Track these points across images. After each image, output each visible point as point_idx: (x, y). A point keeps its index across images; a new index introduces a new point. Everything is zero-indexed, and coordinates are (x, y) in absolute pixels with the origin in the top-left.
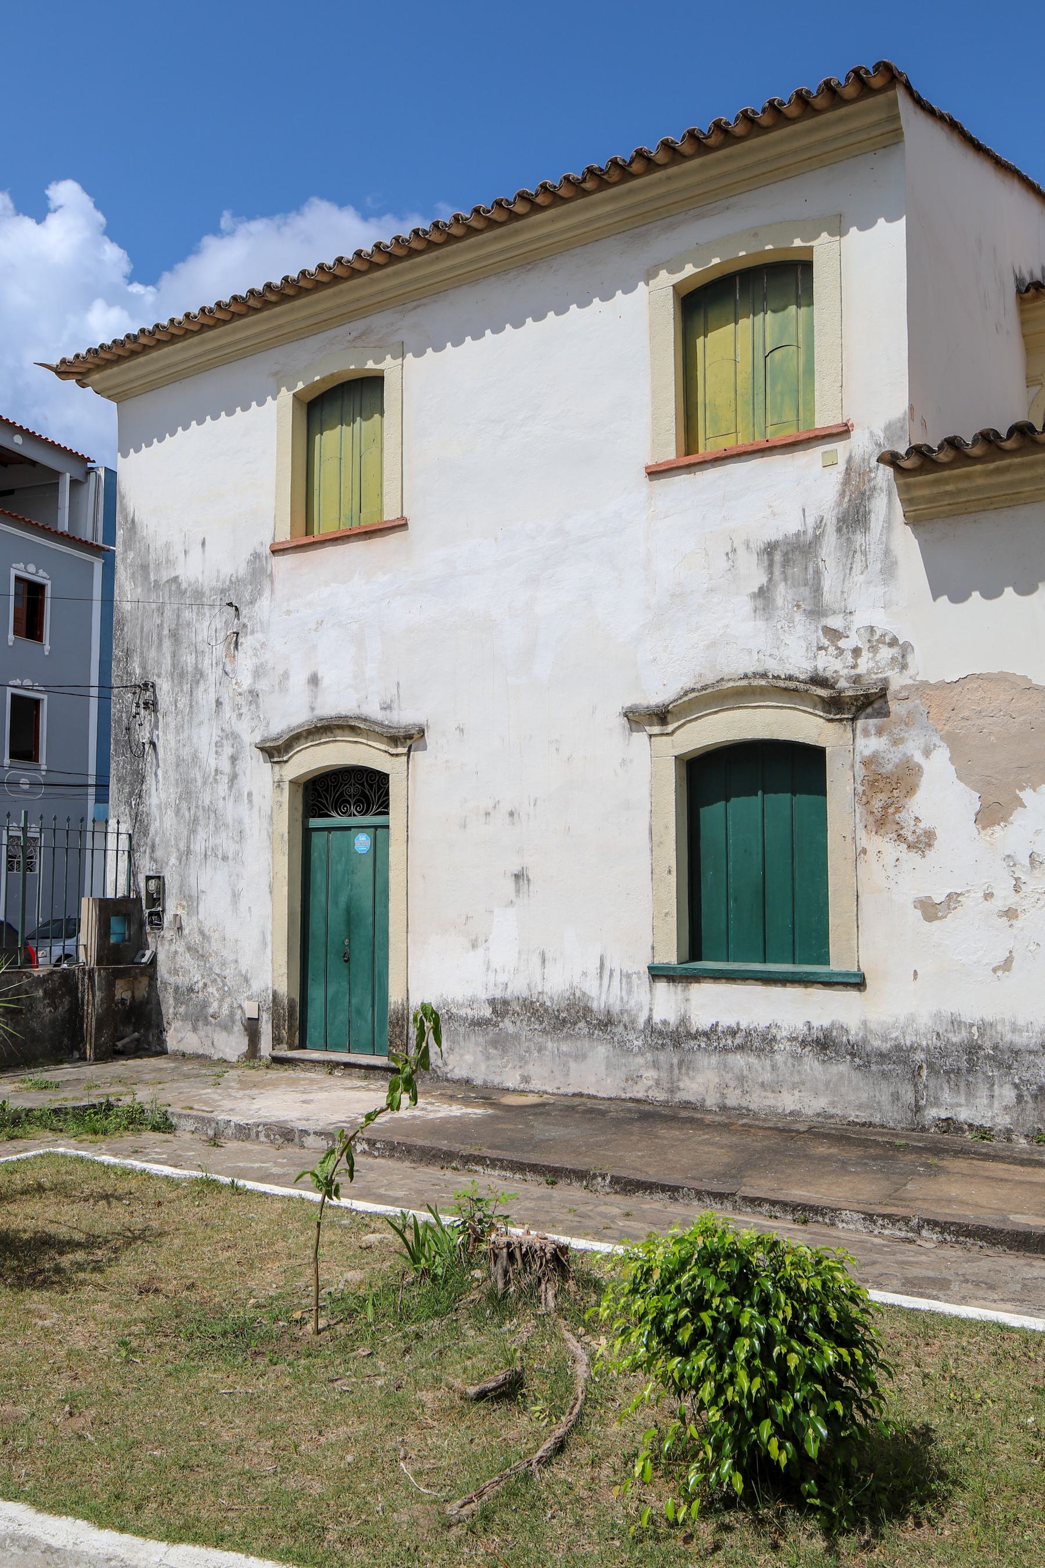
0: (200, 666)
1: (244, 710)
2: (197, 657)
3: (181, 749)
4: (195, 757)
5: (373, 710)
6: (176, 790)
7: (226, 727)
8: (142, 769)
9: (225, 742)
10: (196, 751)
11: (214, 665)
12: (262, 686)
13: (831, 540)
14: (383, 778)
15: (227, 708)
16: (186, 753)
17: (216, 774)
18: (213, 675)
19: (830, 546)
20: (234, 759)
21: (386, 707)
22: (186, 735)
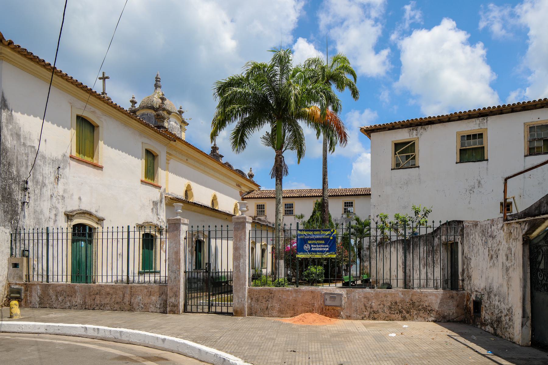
0: (44, 182)
1: (60, 201)
2: (43, 178)
3: (36, 207)
4: (42, 212)
5: (93, 211)
6: (34, 221)
7: (54, 204)
8: (17, 210)
9: (53, 209)
10: (42, 209)
11: (50, 183)
12: (66, 195)
13: (159, 204)
14: (91, 229)
15: (54, 199)
16: (38, 209)
17: (49, 219)
18: (50, 186)
19: (159, 204)
20: (56, 215)
21: (96, 211)
22: (38, 203)
